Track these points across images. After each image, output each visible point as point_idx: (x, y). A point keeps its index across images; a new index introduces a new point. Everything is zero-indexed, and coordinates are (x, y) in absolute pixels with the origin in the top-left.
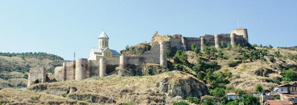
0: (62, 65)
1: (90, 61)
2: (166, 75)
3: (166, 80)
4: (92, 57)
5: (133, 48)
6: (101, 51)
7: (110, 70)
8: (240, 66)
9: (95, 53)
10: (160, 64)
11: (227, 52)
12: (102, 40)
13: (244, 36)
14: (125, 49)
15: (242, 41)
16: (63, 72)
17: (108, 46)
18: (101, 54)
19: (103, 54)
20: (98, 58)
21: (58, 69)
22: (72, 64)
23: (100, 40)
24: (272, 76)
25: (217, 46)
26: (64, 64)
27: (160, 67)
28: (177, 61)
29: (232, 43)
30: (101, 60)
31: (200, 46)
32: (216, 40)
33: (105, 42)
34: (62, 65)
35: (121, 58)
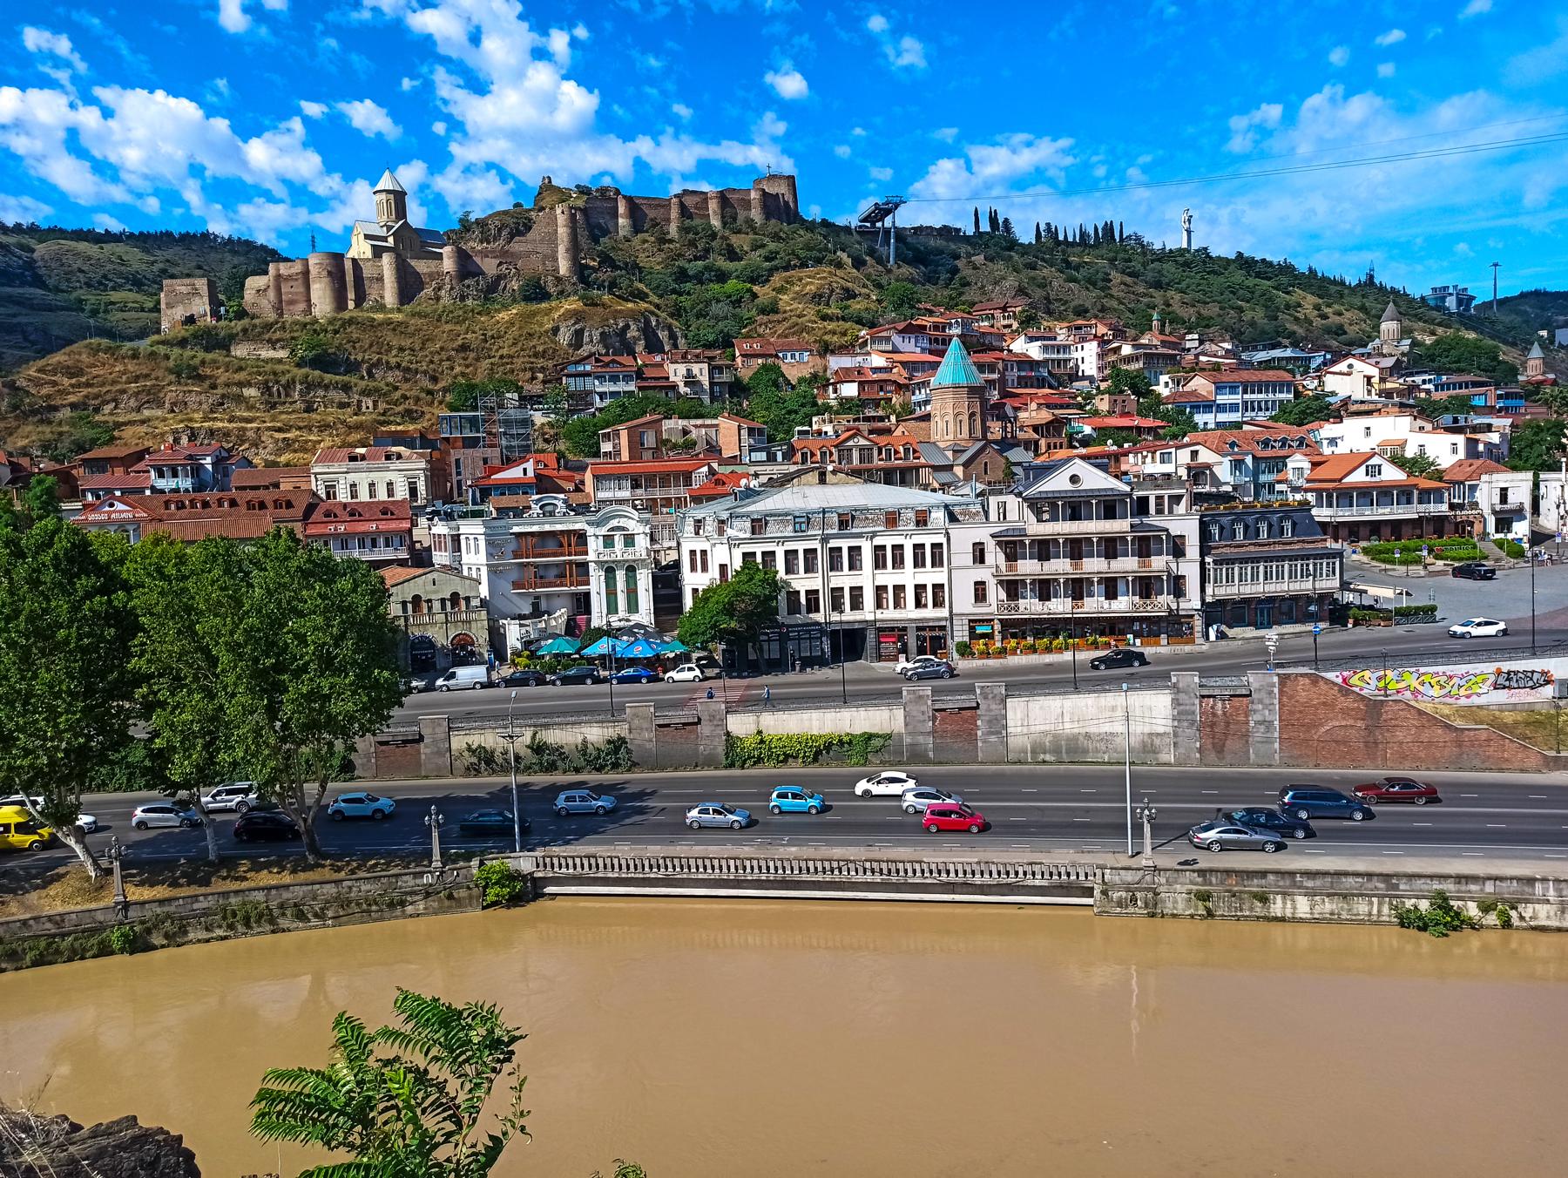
0: (266, 273)
1: (354, 260)
2: (572, 304)
3: (577, 316)
4: (360, 249)
5: (481, 223)
6: (383, 232)
7: (409, 285)
8: (777, 279)
9: (367, 237)
10: (557, 270)
11: (740, 241)
12: (383, 196)
13: (789, 198)
14: (457, 227)
15: (780, 209)
16: (271, 294)
17: (405, 216)
18: (385, 239)
19: (391, 239)
20: (378, 252)
21: (253, 283)
22: (297, 268)
23: (378, 197)
24: (857, 306)
25: (715, 222)
26: (272, 267)
27: (559, 279)
28: (606, 260)
29: (756, 214)
30: (387, 260)
31: (668, 220)
32: (713, 206)
34: (266, 273)
35: (447, 251)
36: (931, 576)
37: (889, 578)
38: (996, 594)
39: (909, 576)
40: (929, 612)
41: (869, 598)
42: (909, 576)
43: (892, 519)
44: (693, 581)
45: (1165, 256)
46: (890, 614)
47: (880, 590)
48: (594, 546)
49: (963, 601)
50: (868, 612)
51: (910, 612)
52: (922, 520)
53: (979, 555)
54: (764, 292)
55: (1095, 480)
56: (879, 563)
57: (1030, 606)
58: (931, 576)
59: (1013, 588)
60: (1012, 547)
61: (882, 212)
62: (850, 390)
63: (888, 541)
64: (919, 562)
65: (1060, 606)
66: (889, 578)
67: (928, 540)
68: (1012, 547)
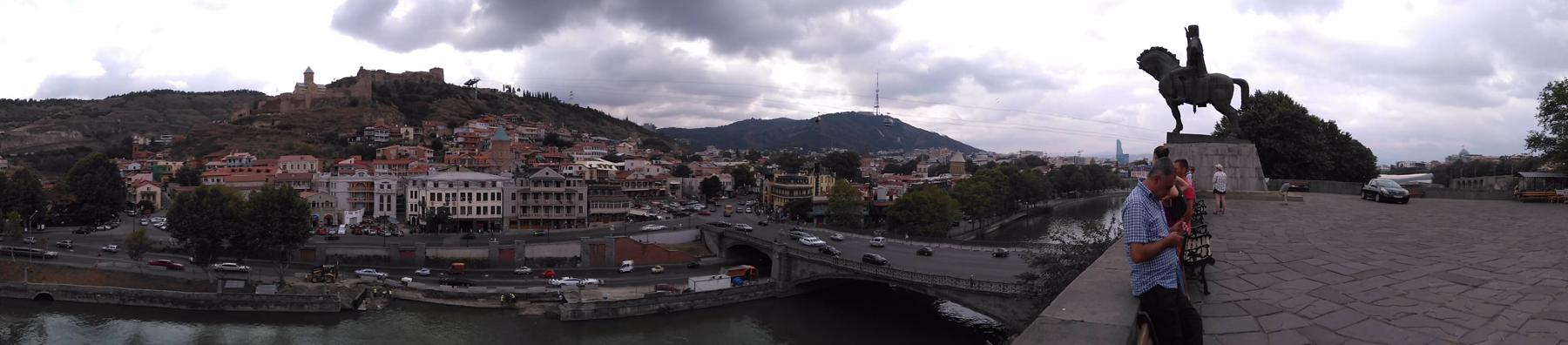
36: (497, 203)
37: (482, 204)
38: (519, 211)
39: (489, 203)
41: (474, 210)
42: (489, 203)
43: (483, 184)
44: (410, 201)
45: (564, 105)
46: (482, 216)
48: (377, 187)
49: (508, 213)
50: (474, 215)
51: (489, 215)
52: (494, 185)
53: (514, 197)
54: (431, 106)
55: (553, 174)
57: (531, 215)
58: (497, 203)
59: (524, 209)
60: (525, 195)
61: (475, 82)
62: (460, 140)
63: (482, 192)
66: (482, 204)
67: (496, 191)
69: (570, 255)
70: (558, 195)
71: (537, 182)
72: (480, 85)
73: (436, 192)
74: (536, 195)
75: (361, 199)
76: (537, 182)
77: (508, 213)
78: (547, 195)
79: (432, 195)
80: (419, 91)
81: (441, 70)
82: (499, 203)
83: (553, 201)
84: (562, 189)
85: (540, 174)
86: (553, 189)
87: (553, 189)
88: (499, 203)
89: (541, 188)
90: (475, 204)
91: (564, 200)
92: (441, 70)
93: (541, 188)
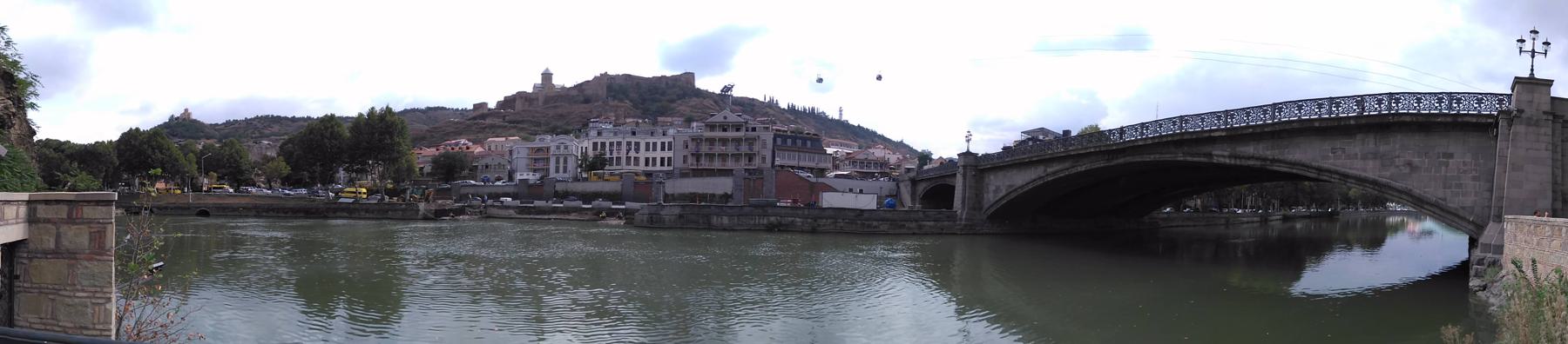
33: (547, 76)
36: (667, 154)
40: (666, 168)
41: (642, 162)
42: (659, 154)
47: (647, 160)
48: (553, 149)
51: (658, 167)
56: (647, 149)
57: (705, 164)
59: (697, 156)
61: (728, 89)
63: (651, 140)
64: (663, 149)
65: (717, 165)
66: (651, 155)
67: (666, 140)
68: (697, 140)
69: (720, 192)
70: (738, 141)
71: (712, 127)
72: (736, 93)
73: (599, 140)
74: (711, 141)
75: (540, 165)
76: (712, 127)
77: (679, 163)
78: (724, 141)
79: (595, 144)
80: (663, 94)
81: (692, 75)
82: (670, 154)
83: (731, 149)
84: (741, 134)
85: (718, 118)
86: (731, 134)
87: (731, 134)
88: (670, 154)
89: (719, 134)
90: (643, 155)
91: (744, 148)
92: (692, 75)
93: (719, 134)
